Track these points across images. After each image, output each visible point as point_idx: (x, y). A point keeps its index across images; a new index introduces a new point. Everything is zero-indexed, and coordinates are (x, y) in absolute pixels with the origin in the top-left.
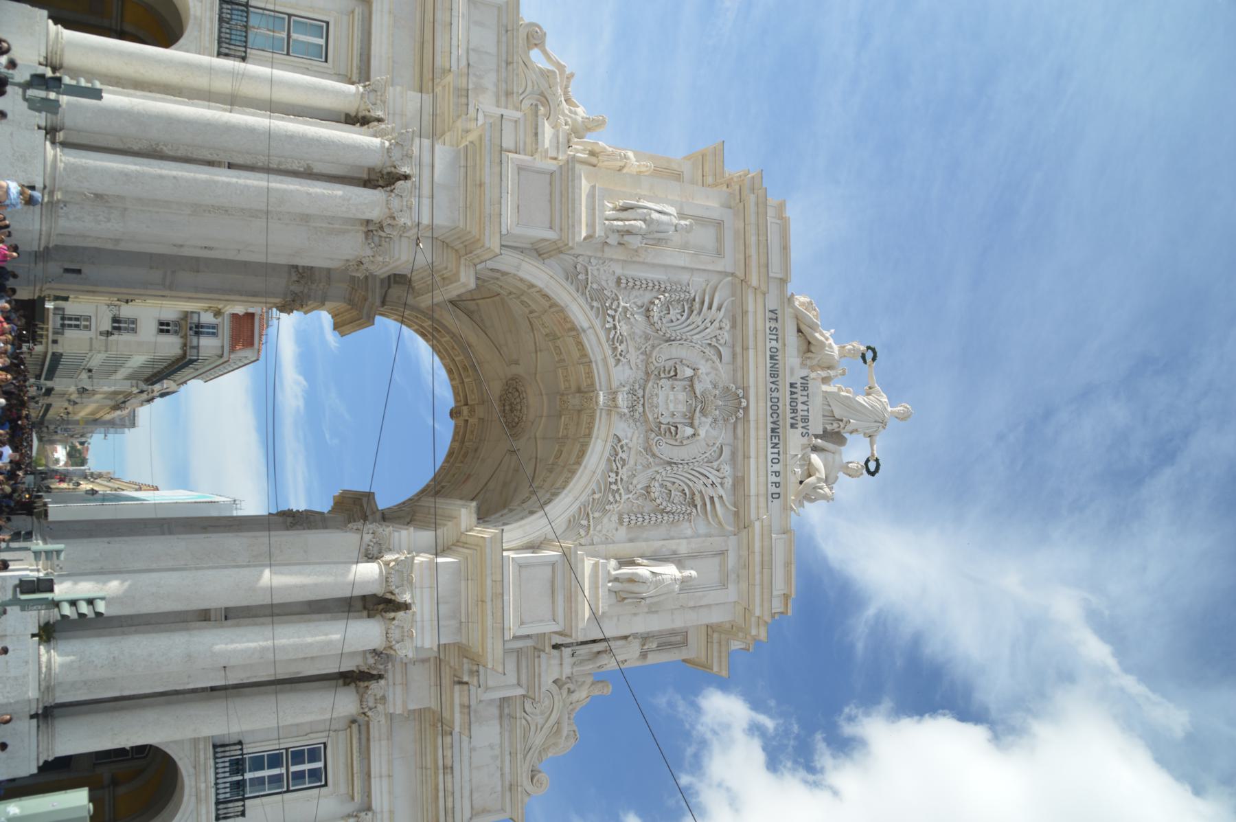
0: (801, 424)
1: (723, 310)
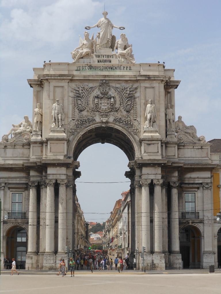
0: (110, 59)
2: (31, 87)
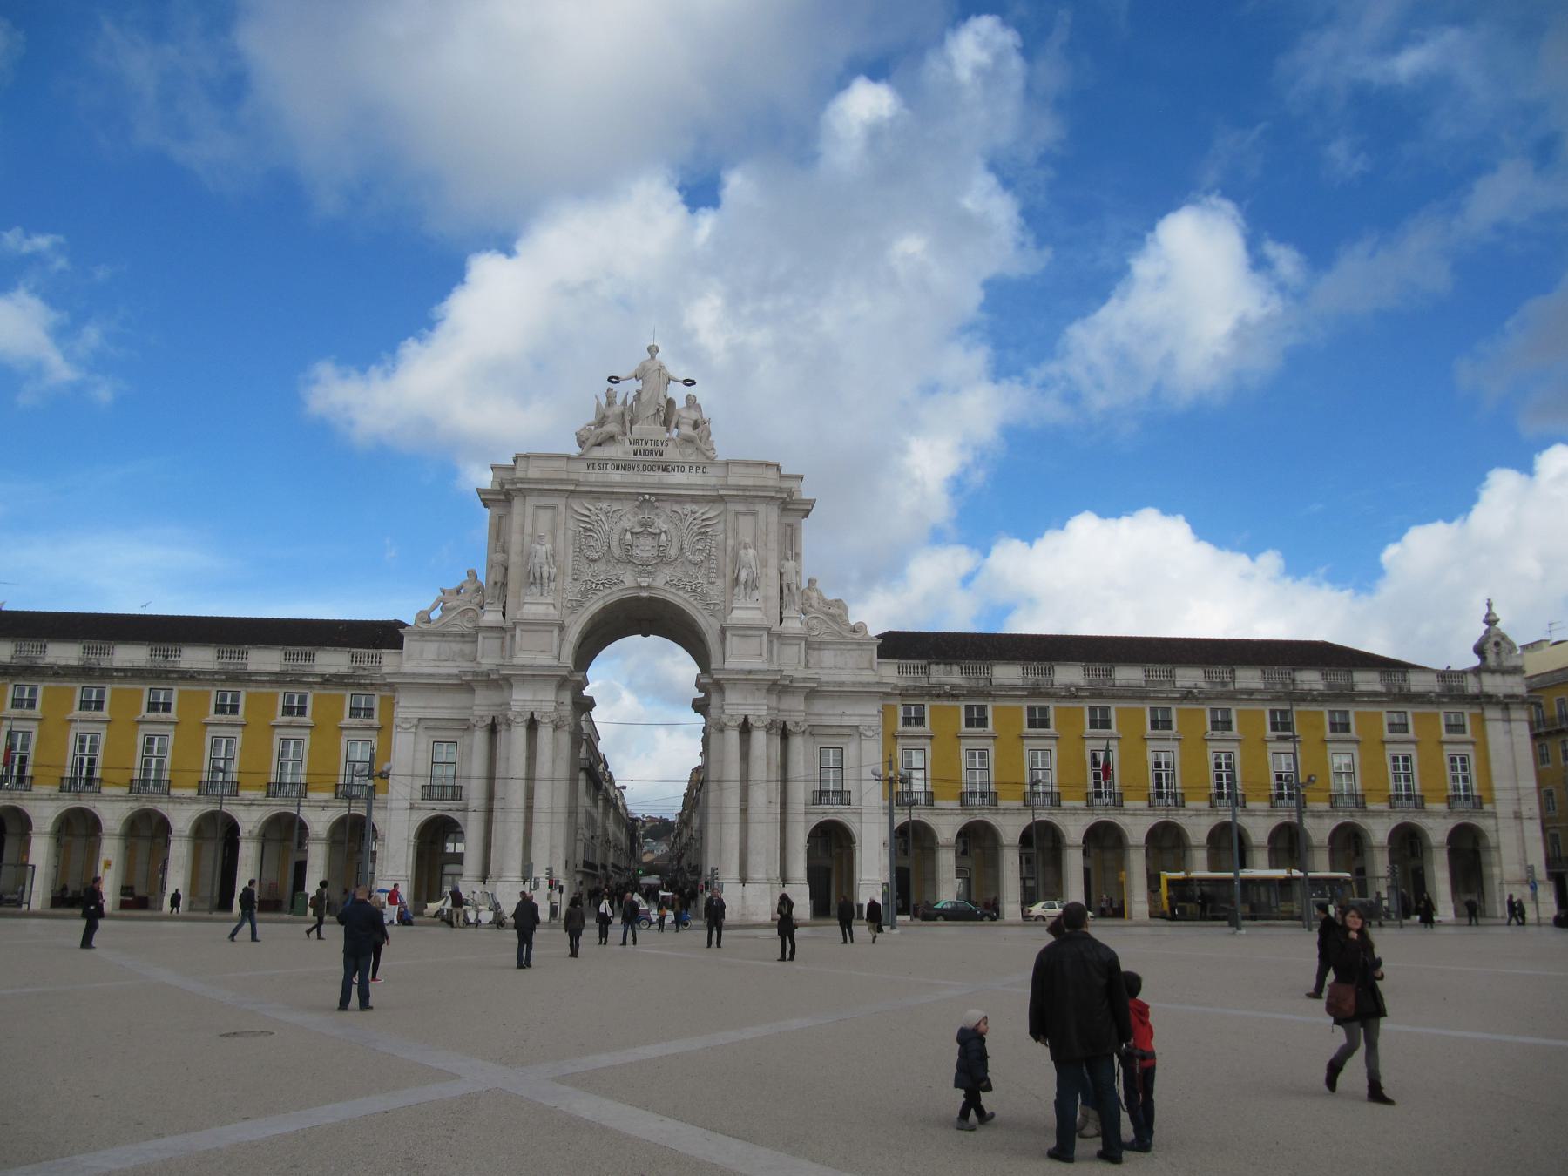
1: (591, 507)
2: (486, 506)
